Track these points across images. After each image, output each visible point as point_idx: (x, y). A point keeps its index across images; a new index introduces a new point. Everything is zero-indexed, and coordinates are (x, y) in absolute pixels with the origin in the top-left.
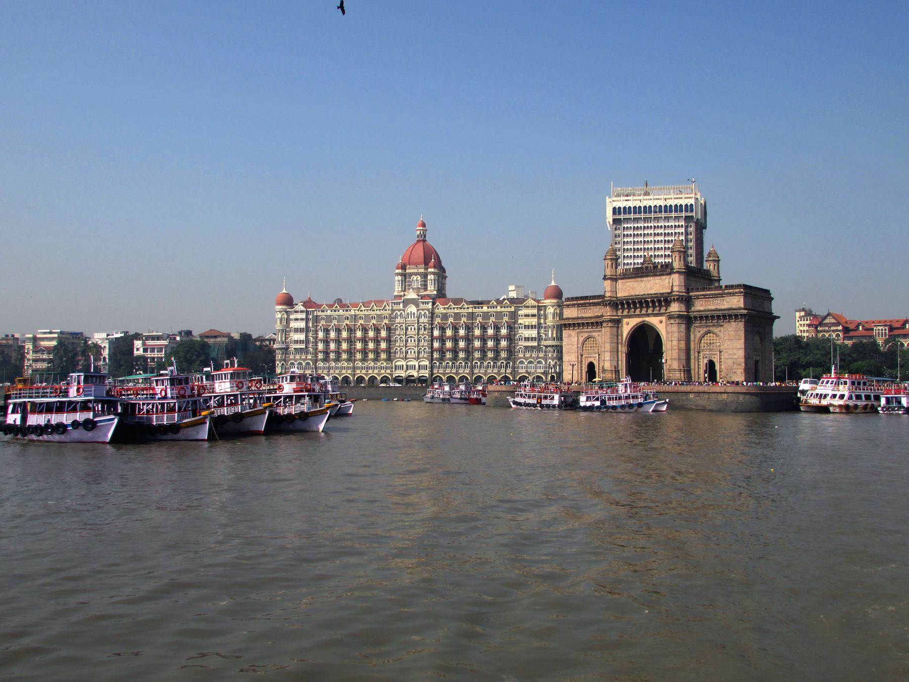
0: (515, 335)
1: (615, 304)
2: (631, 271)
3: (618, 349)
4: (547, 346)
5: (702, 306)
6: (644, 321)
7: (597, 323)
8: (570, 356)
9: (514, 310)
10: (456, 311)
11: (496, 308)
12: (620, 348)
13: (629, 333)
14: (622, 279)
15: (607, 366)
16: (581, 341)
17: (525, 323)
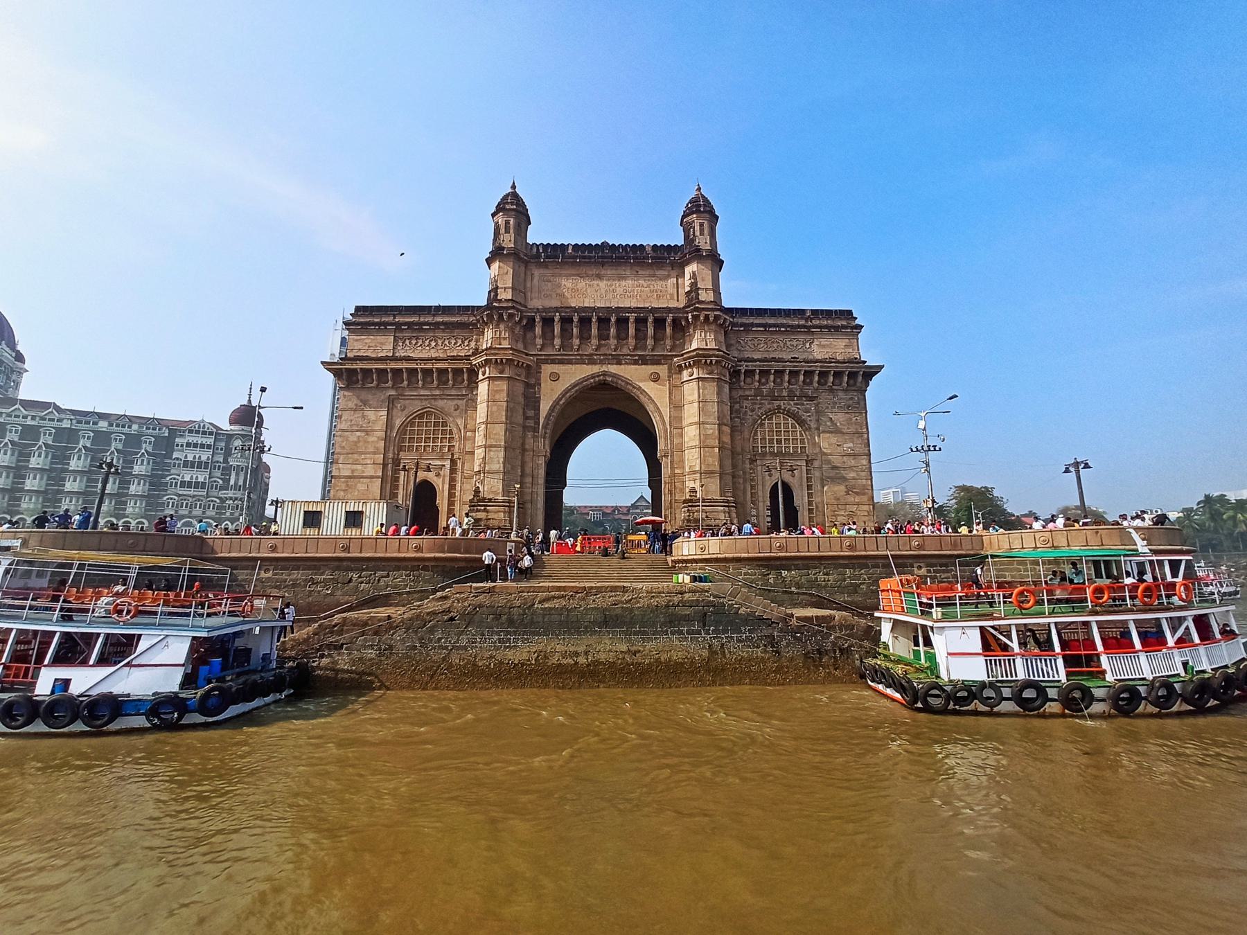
0: (165, 477)
1: (524, 322)
2: (570, 251)
3: (523, 444)
4: (227, 499)
5: (756, 349)
6: (605, 374)
7: (458, 372)
8: (356, 462)
9: (167, 435)
10: (29, 422)
11: (130, 427)
12: (530, 441)
13: (556, 402)
14: (545, 265)
15: (493, 487)
16: (398, 423)
17: (186, 456)
